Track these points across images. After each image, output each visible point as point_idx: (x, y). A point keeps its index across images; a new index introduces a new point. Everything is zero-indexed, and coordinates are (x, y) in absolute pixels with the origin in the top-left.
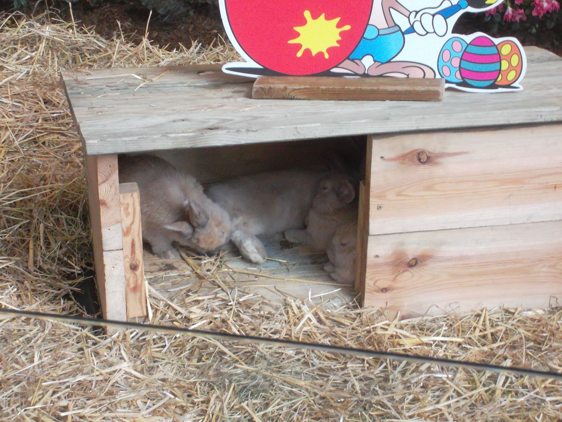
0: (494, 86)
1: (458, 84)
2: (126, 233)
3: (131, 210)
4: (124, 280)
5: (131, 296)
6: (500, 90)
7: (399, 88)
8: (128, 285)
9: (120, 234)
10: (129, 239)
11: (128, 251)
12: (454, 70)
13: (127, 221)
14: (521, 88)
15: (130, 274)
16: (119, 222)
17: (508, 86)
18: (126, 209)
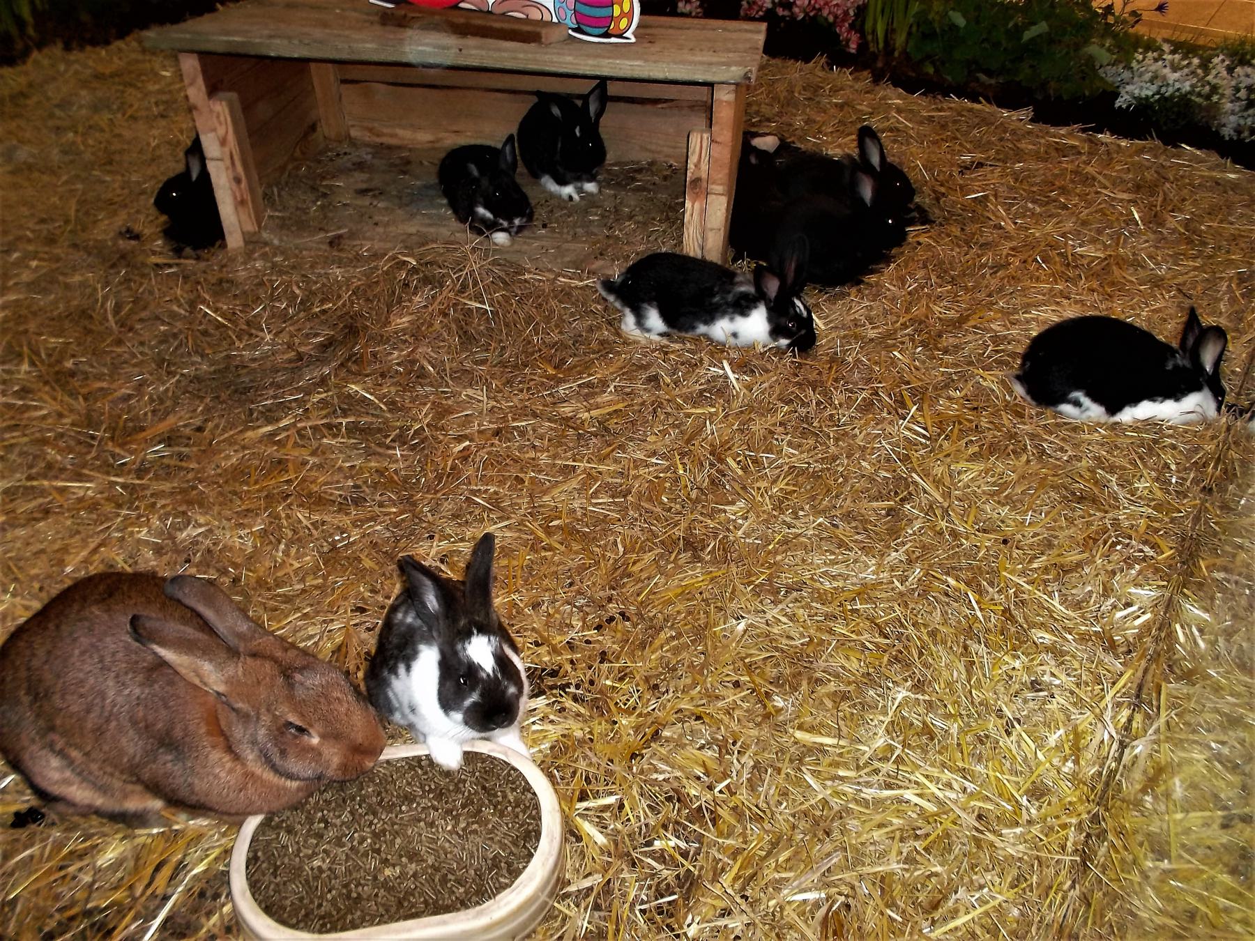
0: (607, 35)
1: (574, 30)
2: (223, 142)
3: (222, 119)
4: (229, 192)
5: (240, 209)
6: (613, 40)
7: (497, 25)
8: (235, 198)
9: (217, 143)
10: (227, 150)
11: (228, 162)
12: (570, 13)
13: (221, 131)
14: (633, 40)
15: (234, 185)
16: (214, 130)
17: (620, 36)
18: (218, 117)
